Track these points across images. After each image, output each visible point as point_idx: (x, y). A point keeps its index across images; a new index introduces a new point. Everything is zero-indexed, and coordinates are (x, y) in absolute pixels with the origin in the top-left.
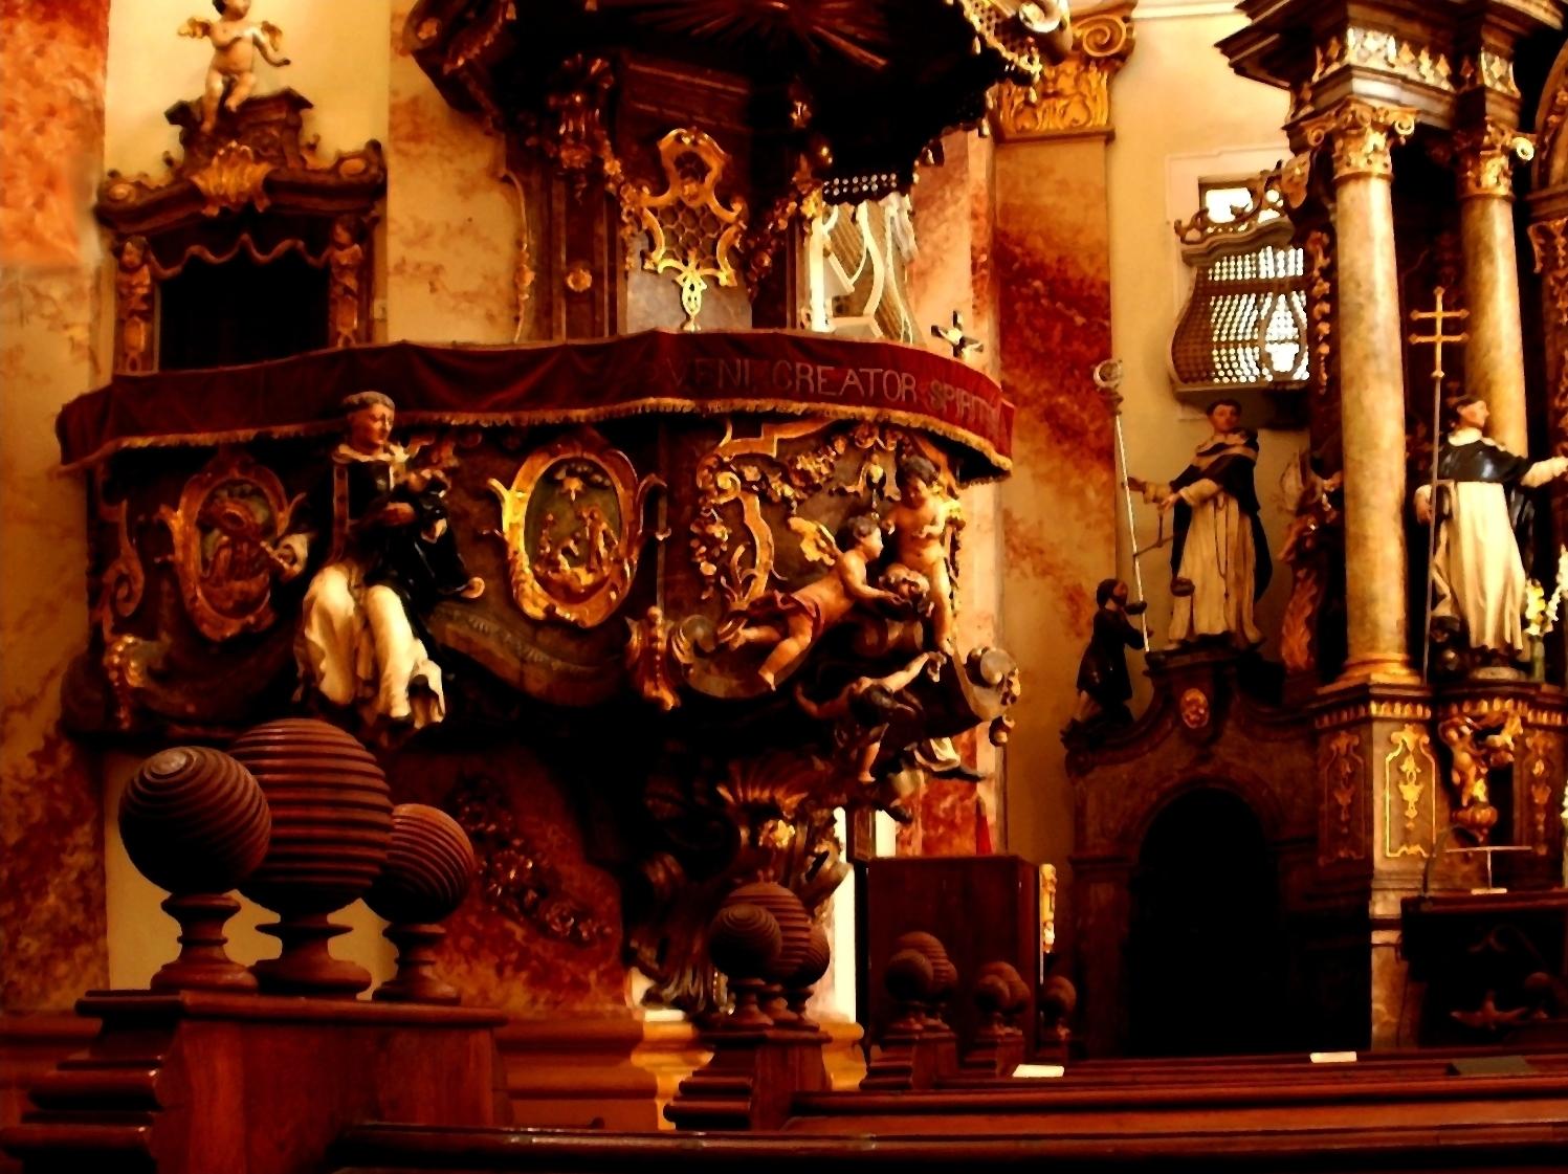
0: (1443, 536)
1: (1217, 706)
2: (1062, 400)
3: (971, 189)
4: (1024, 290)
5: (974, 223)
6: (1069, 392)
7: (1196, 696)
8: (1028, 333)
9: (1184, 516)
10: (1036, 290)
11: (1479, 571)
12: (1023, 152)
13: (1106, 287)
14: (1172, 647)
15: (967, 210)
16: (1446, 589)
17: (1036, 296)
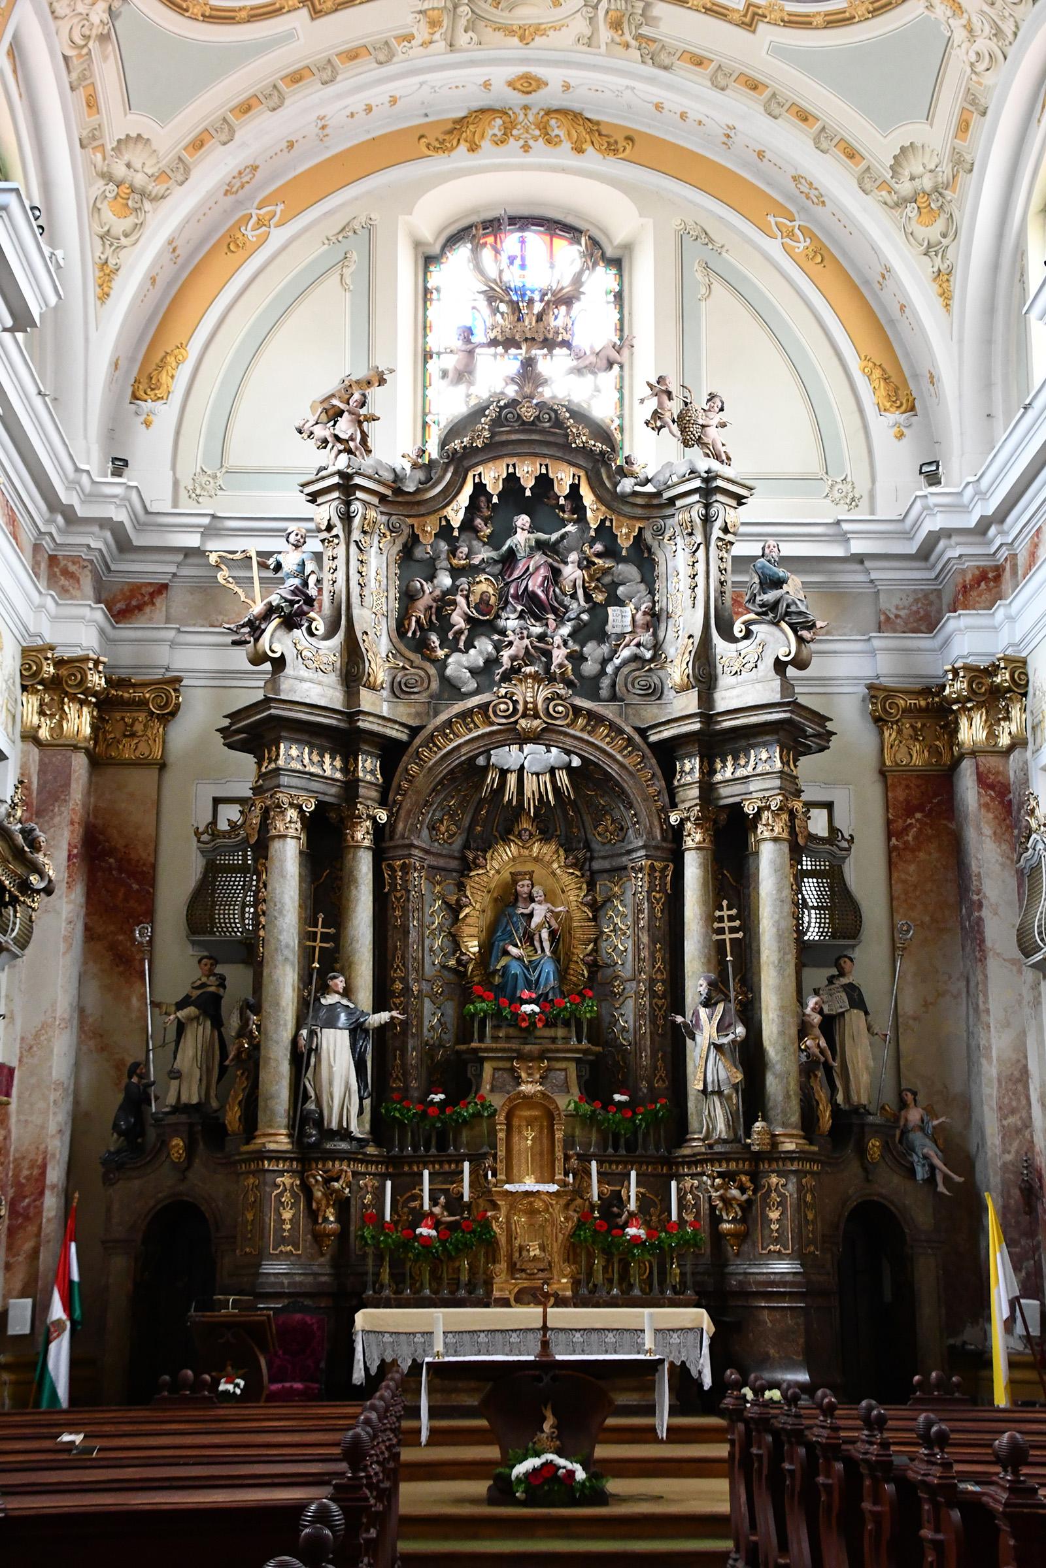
0: (313, 1060)
1: (190, 1149)
2: (121, 938)
3: (71, 805)
4: (103, 864)
5: (71, 828)
6: (125, 933)
7: (178, 1142)
8: (103, 891)
9: (181, 1028)
10: (110, 864)
11: (331, 1084)
12: (111, 771)
13: (154, 867)
14: (167, 1110)
15: (68, 818)
16: (312, 1093)
17: (110, 869)
